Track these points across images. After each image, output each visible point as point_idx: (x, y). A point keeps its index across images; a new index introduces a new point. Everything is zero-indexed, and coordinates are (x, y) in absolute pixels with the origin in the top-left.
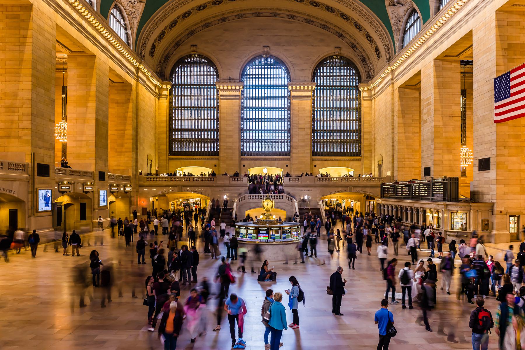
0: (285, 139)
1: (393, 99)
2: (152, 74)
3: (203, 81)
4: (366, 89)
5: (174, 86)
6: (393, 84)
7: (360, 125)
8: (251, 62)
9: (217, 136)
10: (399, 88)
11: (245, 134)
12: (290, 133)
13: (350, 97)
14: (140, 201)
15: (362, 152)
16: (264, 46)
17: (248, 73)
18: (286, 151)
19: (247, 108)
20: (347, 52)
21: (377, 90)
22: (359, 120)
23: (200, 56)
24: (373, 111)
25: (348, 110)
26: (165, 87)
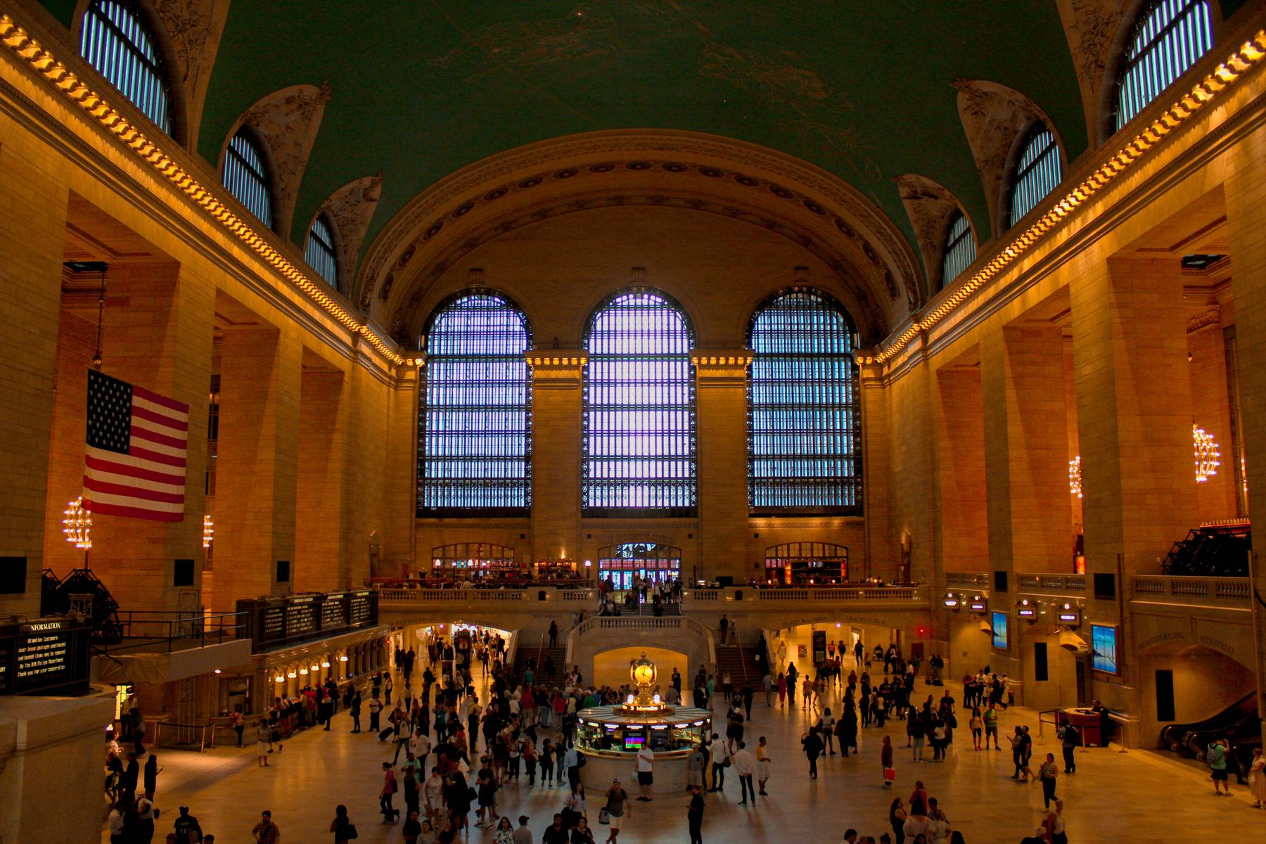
0: (683, 478)
3: (498, 347)
4: (869, 361)
5: (430, 359)
6: (926, 359)
8: (604, 303)
9: (527, 472)
10: (940, 373)
11: (592, 464)
12: (695, 461)
15: (865, 507)
16: (634, 269)
17: (599, 328)
18: (687, 504)
21: (894, 366)
23: (489, 293)
26: (410, 362)
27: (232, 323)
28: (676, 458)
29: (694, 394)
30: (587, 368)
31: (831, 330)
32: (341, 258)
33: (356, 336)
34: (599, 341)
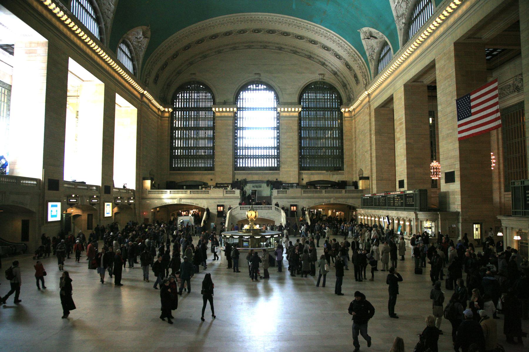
1: (370, 120)
2: (155, 100)
3: (202, 105)
4: (347, 110)
5: (175, 109)
6: (370, 106)
7: (342, 143)
8: (244, 88)
9: (213, 152)
11: (239, 151)
13: (333, 118)
14: (143, 212)
17: (241, 97)
19: (240, 127)
20: (329, 78)
22: (341, 137)
24: (353, 130)
25: (331, 129)
26: (166, 110)
27: (83, 81)
28: (272, 148)
29: (279, 123)
30: (236, 113)
31: (332, 99)
32: (136, 63)
33: (143, 95)
34: (241, 103)
